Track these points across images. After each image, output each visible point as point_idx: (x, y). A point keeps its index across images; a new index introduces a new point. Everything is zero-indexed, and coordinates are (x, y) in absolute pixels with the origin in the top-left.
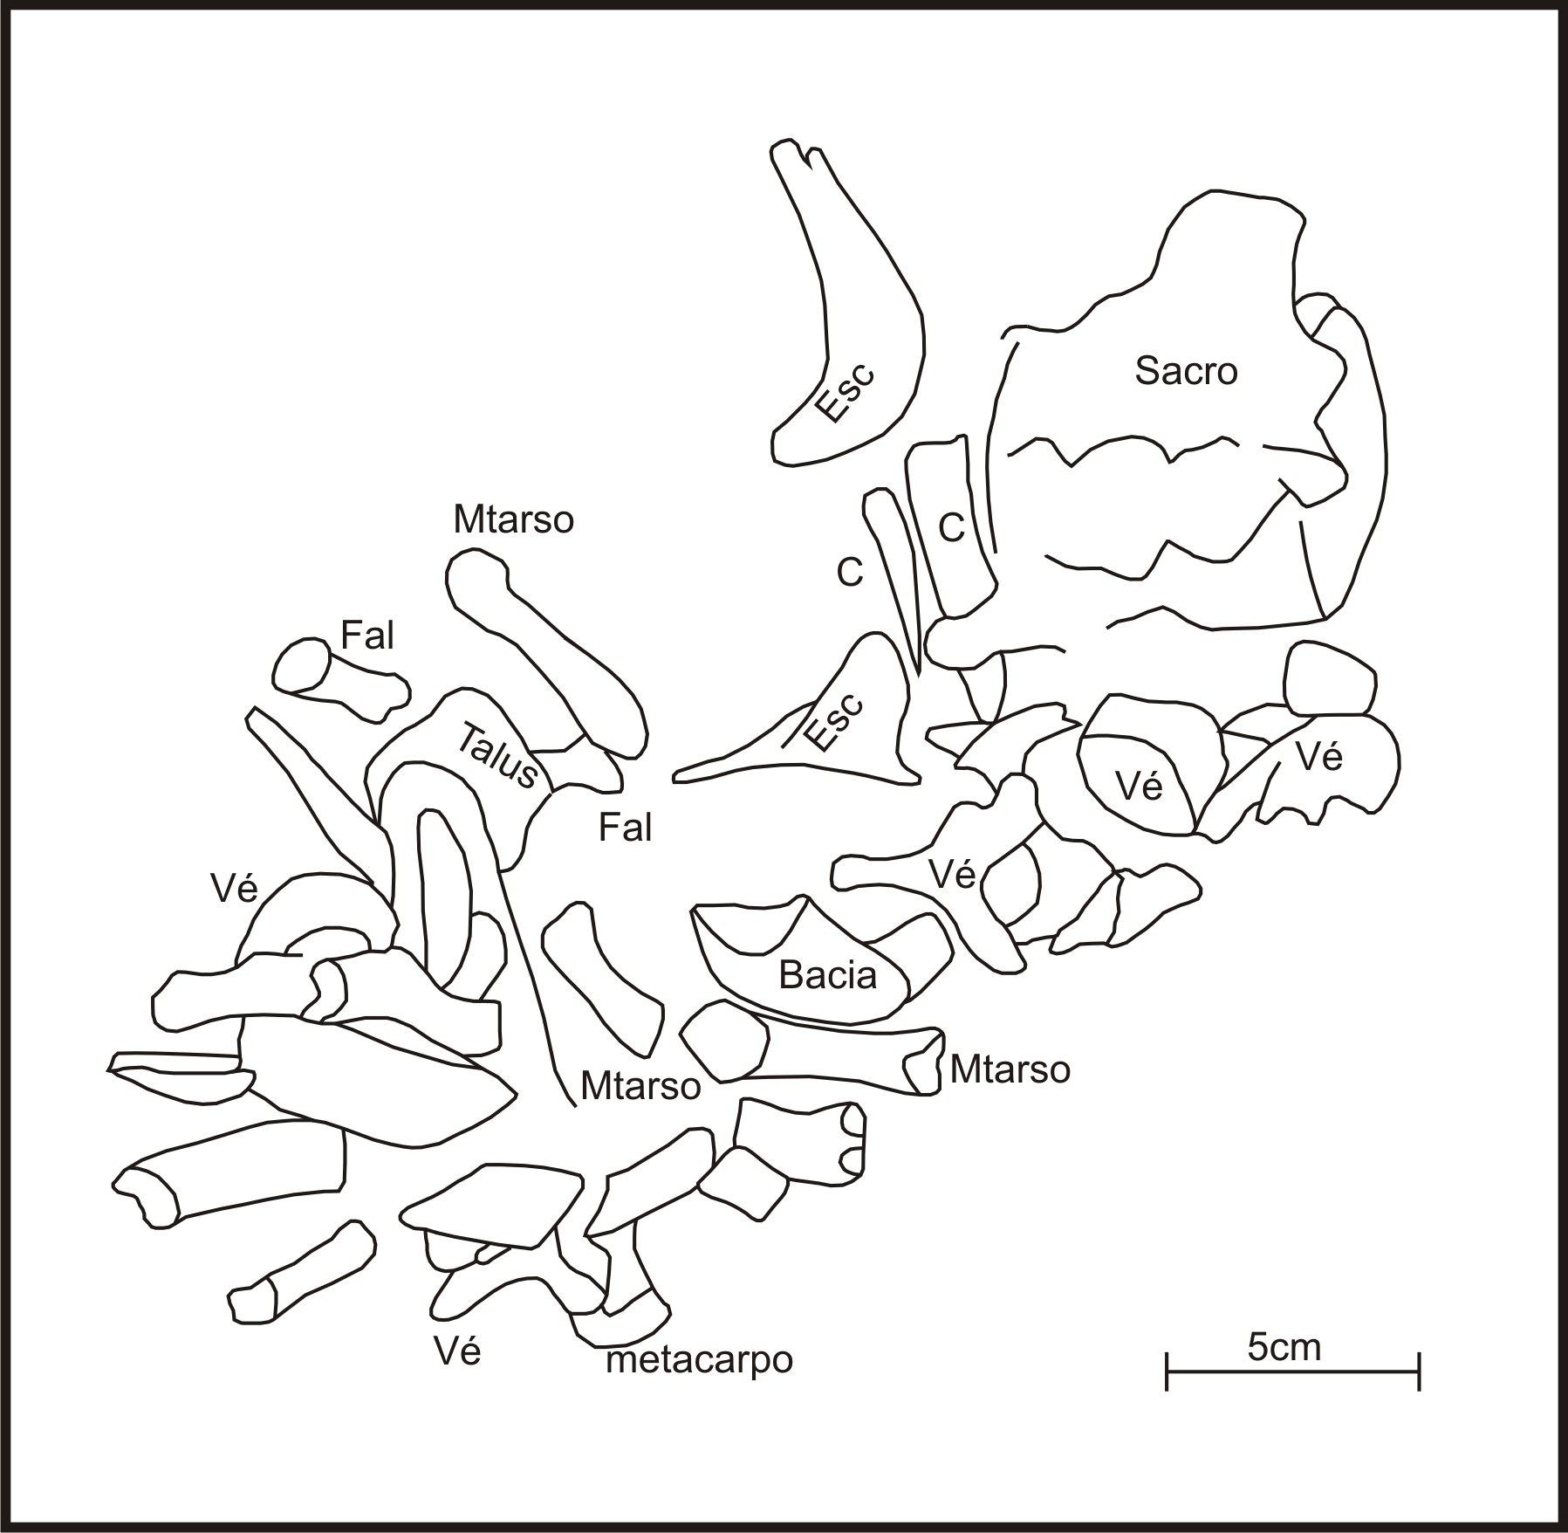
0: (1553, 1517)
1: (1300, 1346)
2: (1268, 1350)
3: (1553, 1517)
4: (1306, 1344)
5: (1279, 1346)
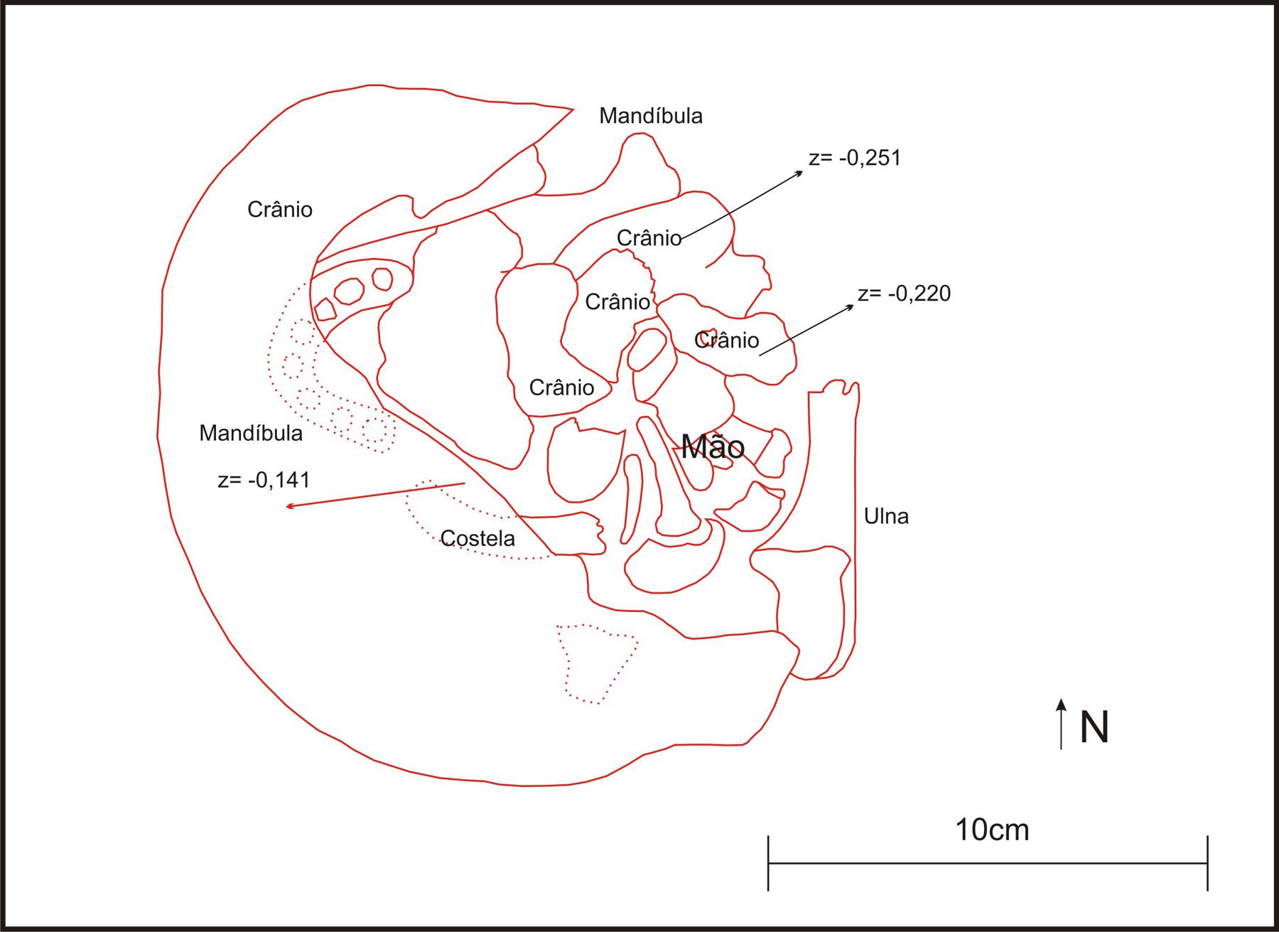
1: (1012, 830)
4: (1017, 827)
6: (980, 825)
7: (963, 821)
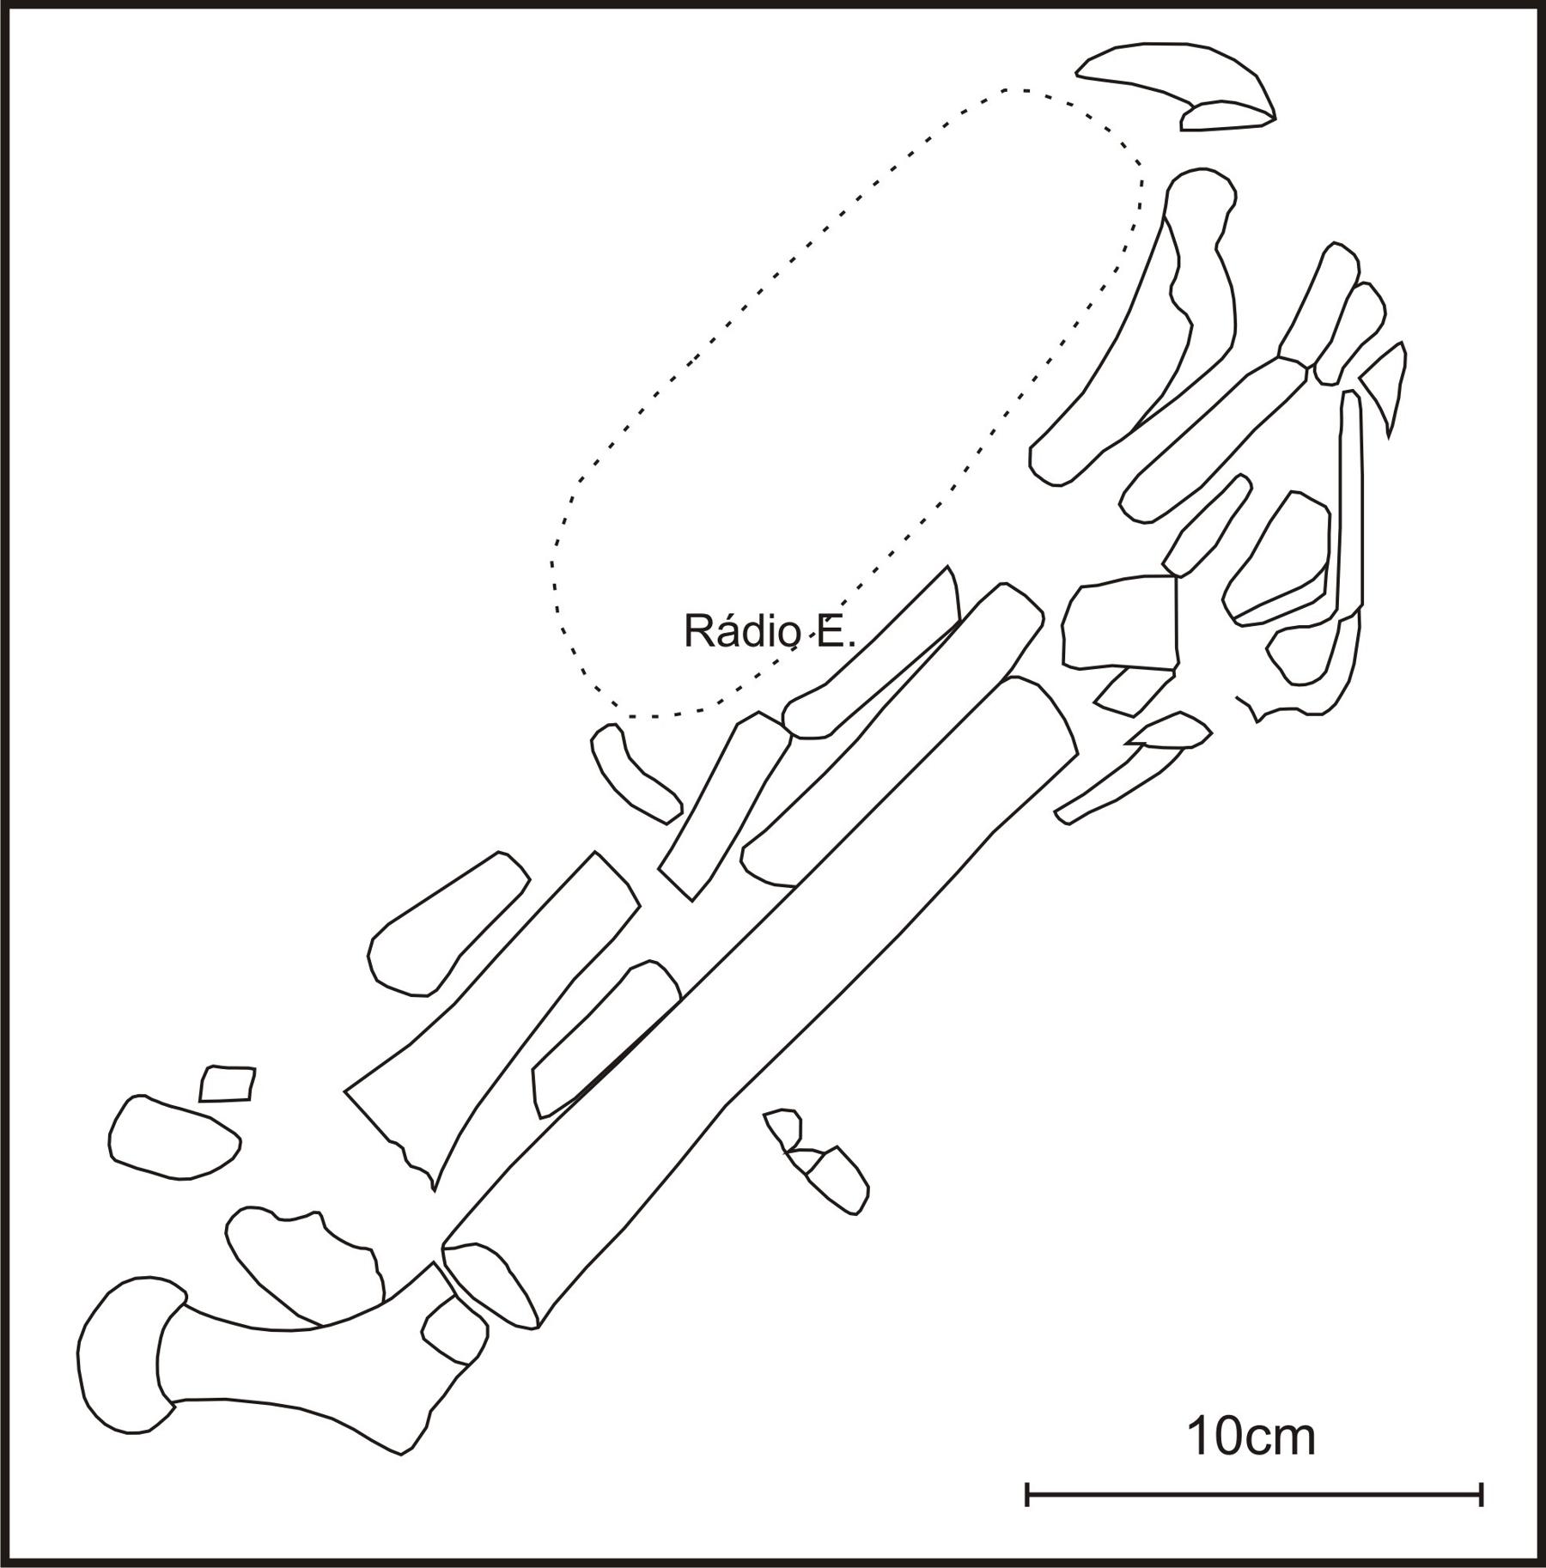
0: (1534, 1555)
1: (1287, 1436)
2: (1245, 1439)
3: (1534, 1555)
4: (1295, 1432)
5: (1258, 1434)
6: (1229, 1426)
7: (1200, 1422)
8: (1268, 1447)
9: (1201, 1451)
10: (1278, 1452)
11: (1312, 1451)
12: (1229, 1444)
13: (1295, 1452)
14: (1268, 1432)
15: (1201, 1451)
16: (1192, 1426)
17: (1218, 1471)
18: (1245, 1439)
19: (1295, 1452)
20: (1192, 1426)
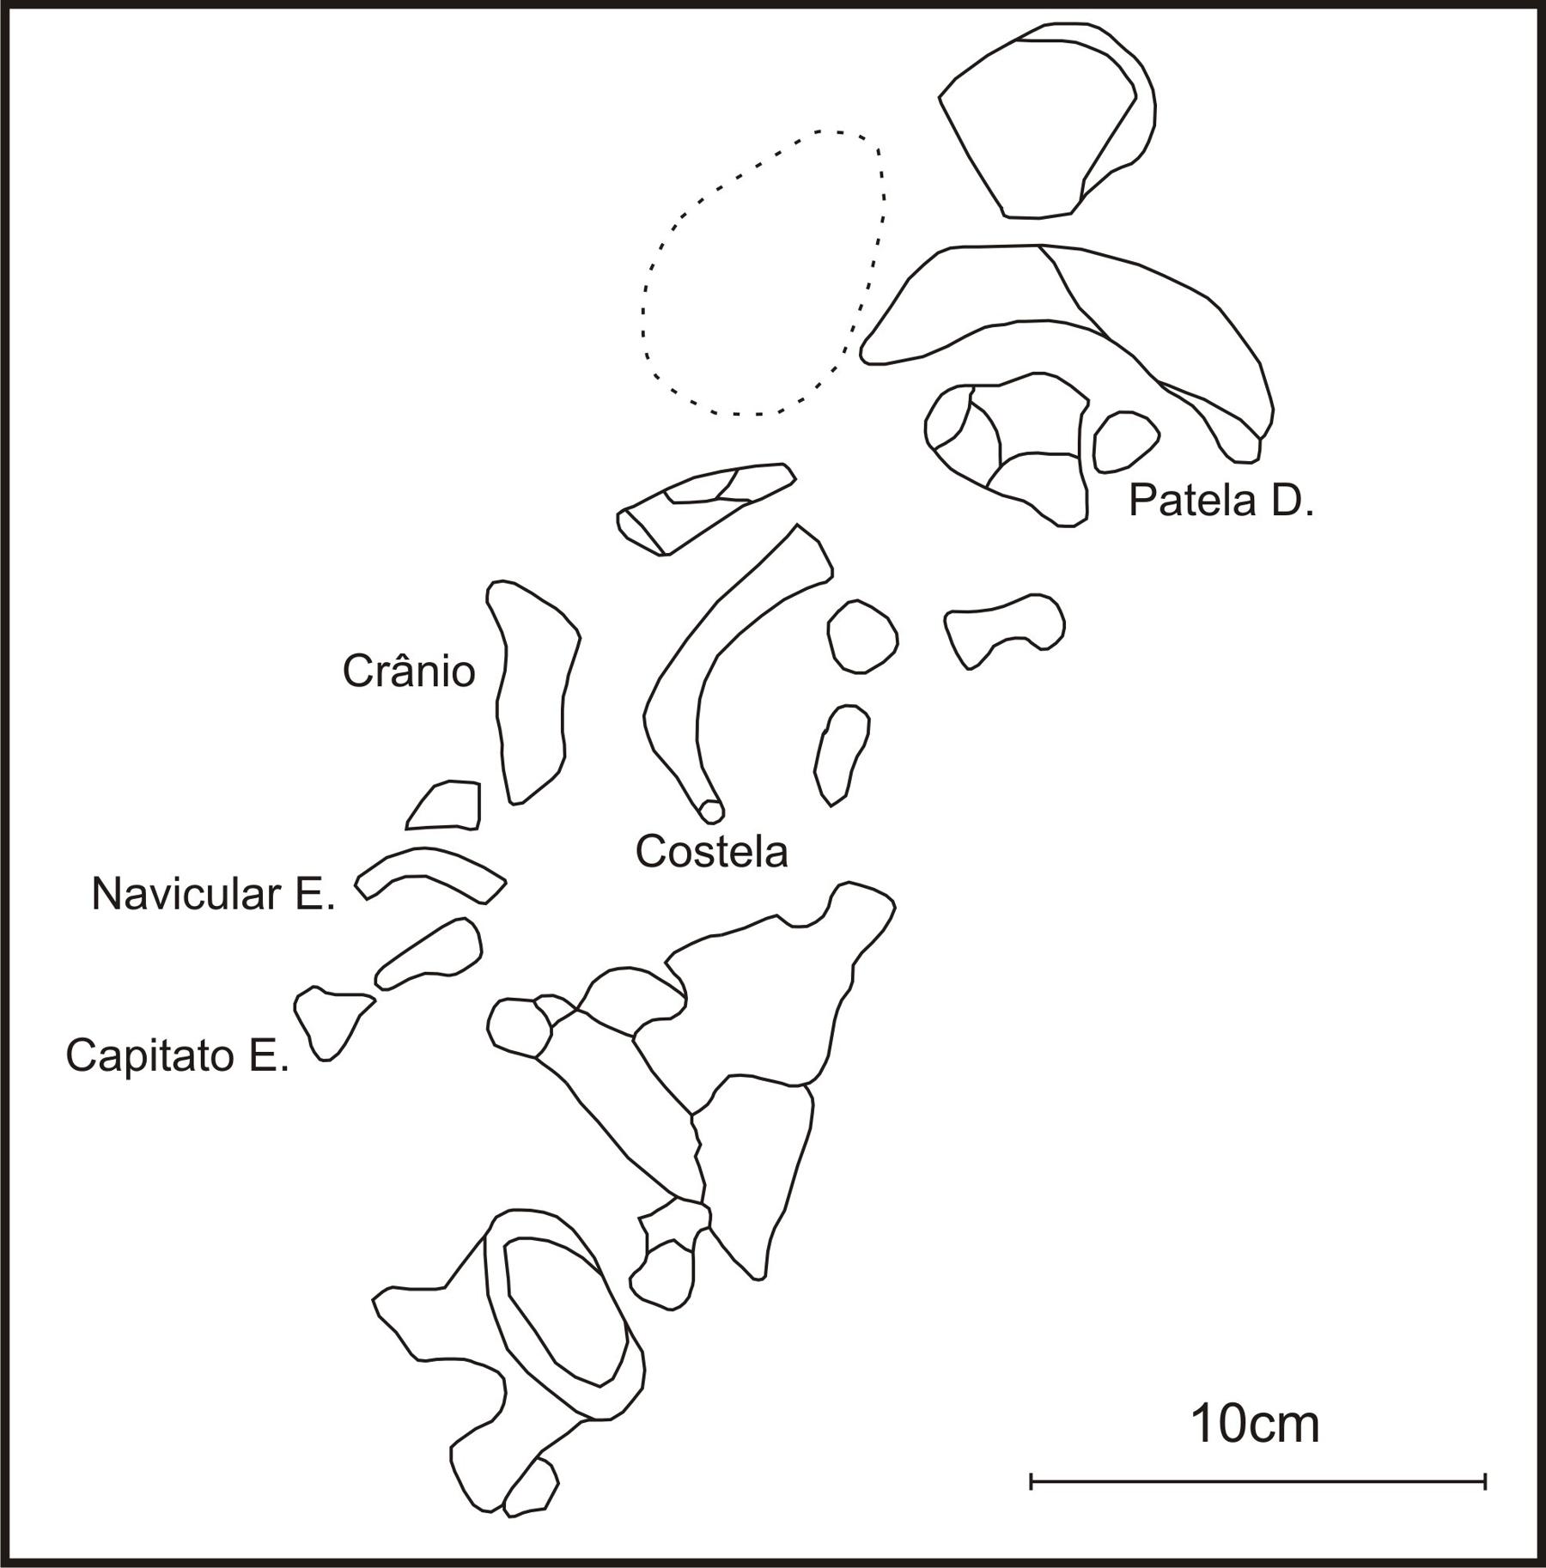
1: (1290, 1424)
2: (1249, 1426)
4: (1299, 1420)
5: (1262, 1421)
6: (1233, 1411)
7: (1204, 1409)
8: (1272, 1434)
9: (1205, 1439)
10: (1282, 1439)
11: (1315, 1439)
12: (1233, 1431)
13: (1299, 1439)
14: (1272, 1419)
15: (1205, 1439)
16: (1196, 1413)
17: (1221, 1458)
18: (1249, 1426)
19: (1299, 1439)
20: (1196, 1413)
